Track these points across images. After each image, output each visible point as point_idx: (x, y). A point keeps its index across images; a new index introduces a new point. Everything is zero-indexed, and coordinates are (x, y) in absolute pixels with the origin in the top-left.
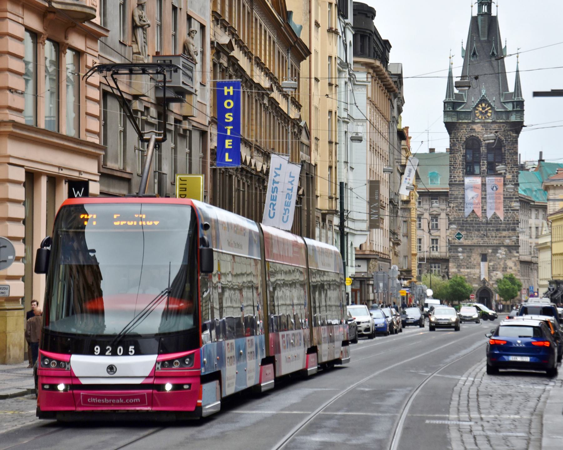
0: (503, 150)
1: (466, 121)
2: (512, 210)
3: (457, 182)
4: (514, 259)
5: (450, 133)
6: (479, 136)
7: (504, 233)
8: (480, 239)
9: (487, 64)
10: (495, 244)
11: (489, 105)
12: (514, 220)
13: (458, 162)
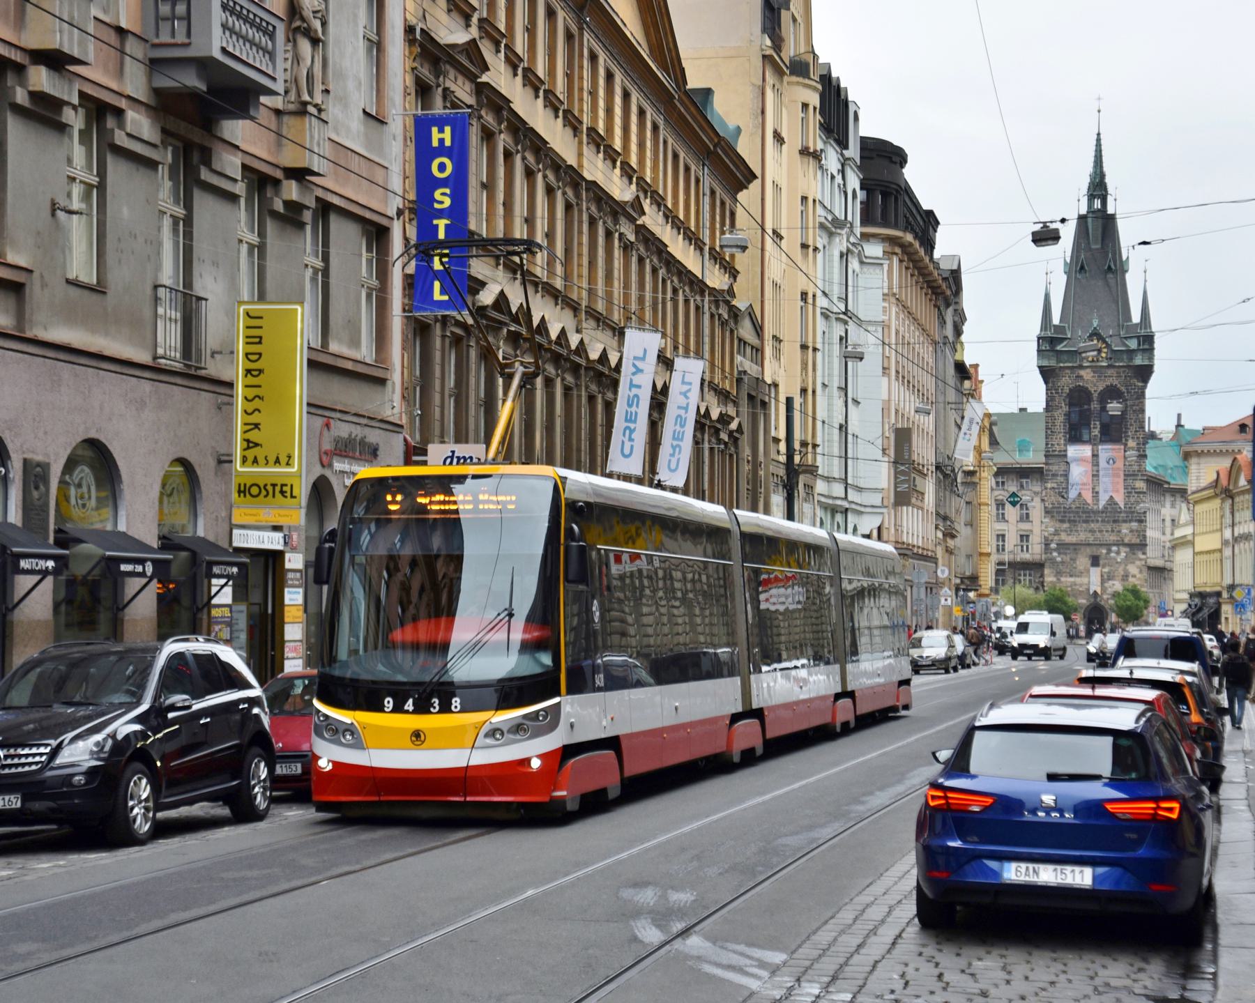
4: (1138, 563)
5: (1046, 382)
6: (1089, 386)
8: (1089, 535)
9: (1100, 283)
11: (1104, 341)
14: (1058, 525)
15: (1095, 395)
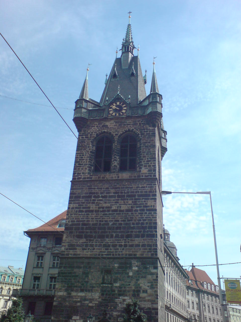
0: (138, 144)
1: (99, 118)
2: (147, 210)
3: (81, 180)
7: (137, 241)
10: (124, 256)
12: (150, 223)
13: (85, 157)
14: (75, 241)
15: (116, 138)
